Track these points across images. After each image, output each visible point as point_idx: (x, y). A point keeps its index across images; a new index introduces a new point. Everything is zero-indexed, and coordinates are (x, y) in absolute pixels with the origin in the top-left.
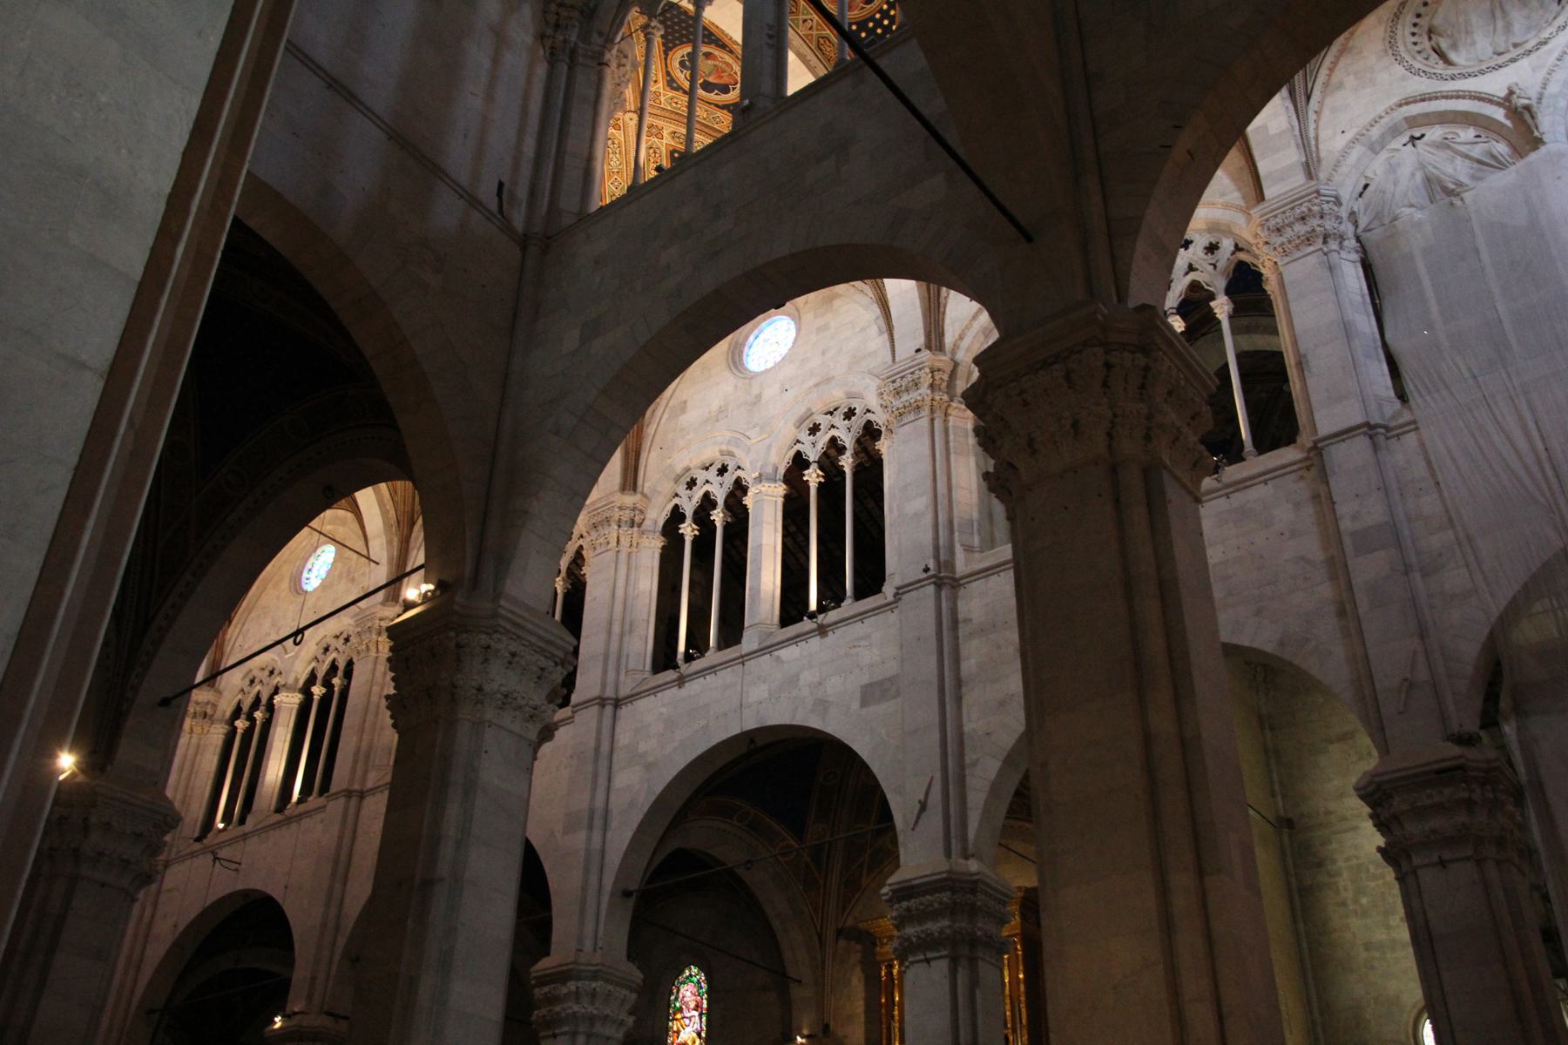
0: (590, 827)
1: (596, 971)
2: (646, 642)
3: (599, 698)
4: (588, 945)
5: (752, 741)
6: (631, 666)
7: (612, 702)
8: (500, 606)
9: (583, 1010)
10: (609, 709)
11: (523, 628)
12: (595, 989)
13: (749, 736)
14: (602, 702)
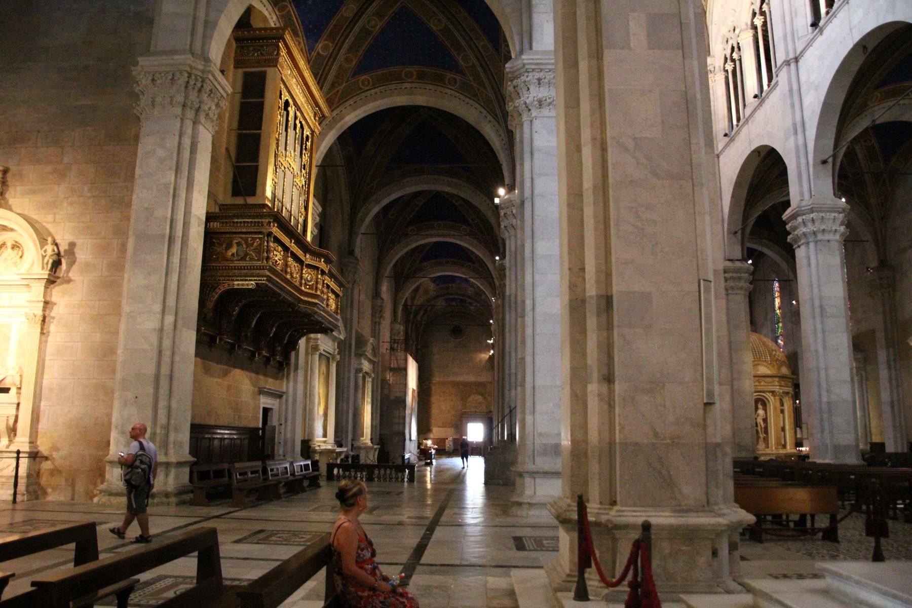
0: (796, 133)
1: (812, 208)
2: (806, 18)
3: (785, 61)
4: (807, 196)
5: (865, 47)
6: (800, 35)
7: (793, 60)
8: (523, 60)
9: (809, 230)
10: (793, 65)
11: (541, 64)
12: (813, 218)
13: (861, 46)
14: (787, 63)
